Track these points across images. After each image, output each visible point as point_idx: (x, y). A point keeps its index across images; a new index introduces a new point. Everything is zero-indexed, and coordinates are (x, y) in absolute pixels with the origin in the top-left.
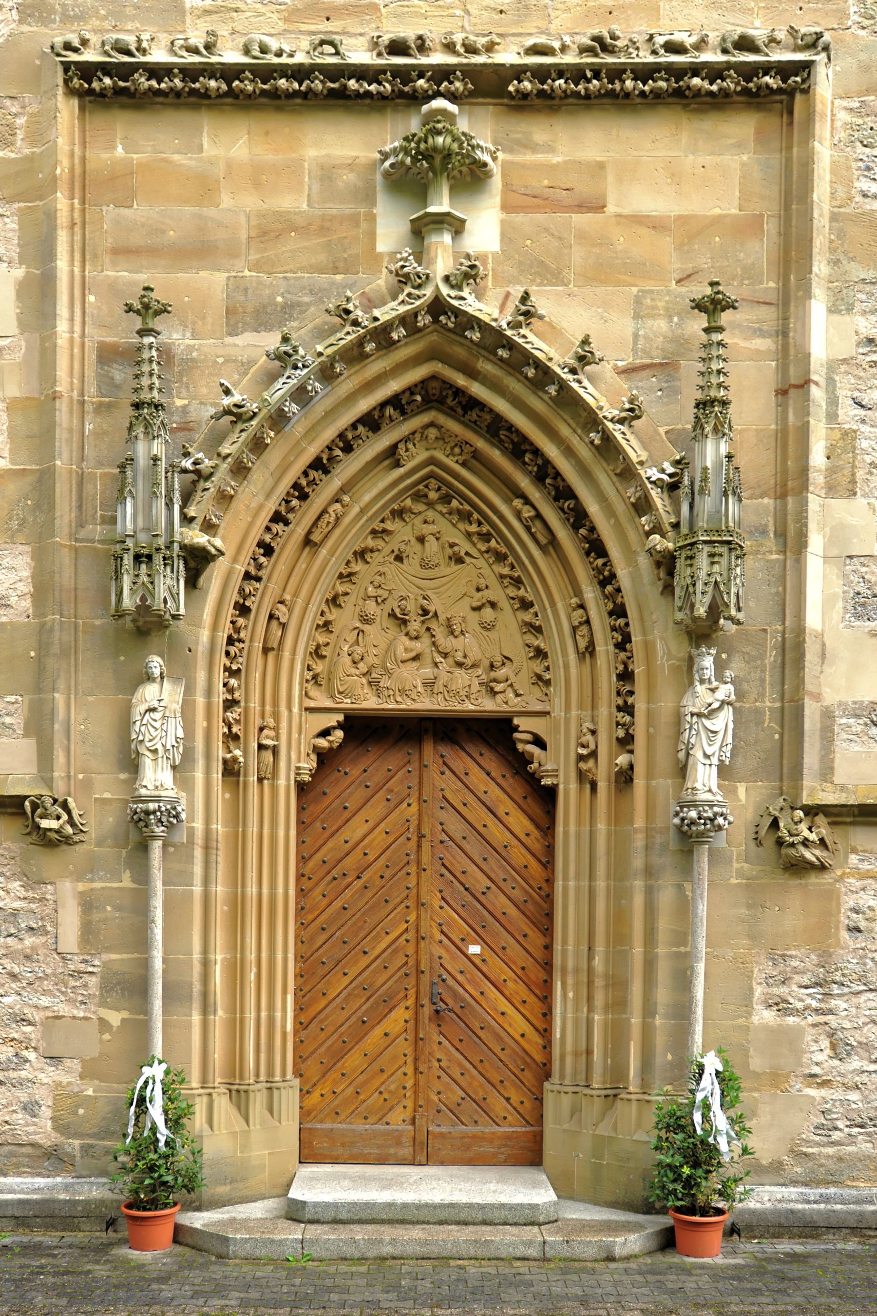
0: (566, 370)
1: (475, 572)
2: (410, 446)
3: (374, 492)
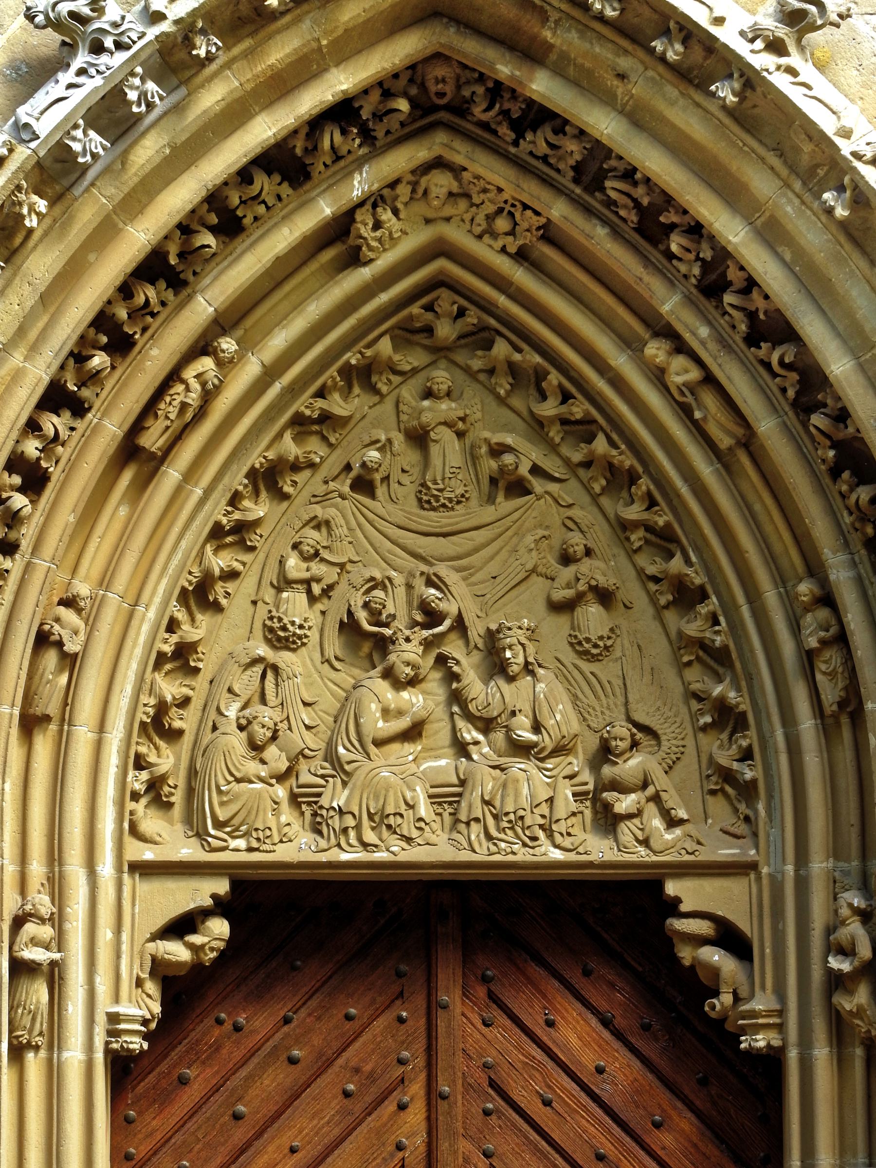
0: (759, 44)
1: (556, 516)
2: (386, 216)
3: (298, 325)
